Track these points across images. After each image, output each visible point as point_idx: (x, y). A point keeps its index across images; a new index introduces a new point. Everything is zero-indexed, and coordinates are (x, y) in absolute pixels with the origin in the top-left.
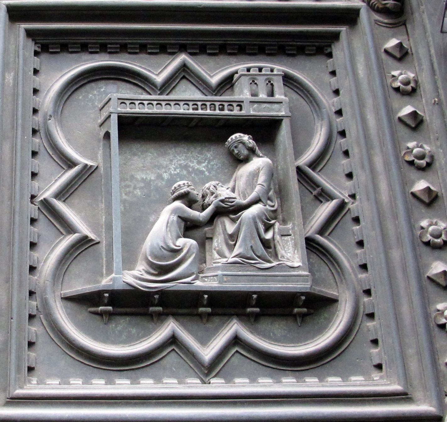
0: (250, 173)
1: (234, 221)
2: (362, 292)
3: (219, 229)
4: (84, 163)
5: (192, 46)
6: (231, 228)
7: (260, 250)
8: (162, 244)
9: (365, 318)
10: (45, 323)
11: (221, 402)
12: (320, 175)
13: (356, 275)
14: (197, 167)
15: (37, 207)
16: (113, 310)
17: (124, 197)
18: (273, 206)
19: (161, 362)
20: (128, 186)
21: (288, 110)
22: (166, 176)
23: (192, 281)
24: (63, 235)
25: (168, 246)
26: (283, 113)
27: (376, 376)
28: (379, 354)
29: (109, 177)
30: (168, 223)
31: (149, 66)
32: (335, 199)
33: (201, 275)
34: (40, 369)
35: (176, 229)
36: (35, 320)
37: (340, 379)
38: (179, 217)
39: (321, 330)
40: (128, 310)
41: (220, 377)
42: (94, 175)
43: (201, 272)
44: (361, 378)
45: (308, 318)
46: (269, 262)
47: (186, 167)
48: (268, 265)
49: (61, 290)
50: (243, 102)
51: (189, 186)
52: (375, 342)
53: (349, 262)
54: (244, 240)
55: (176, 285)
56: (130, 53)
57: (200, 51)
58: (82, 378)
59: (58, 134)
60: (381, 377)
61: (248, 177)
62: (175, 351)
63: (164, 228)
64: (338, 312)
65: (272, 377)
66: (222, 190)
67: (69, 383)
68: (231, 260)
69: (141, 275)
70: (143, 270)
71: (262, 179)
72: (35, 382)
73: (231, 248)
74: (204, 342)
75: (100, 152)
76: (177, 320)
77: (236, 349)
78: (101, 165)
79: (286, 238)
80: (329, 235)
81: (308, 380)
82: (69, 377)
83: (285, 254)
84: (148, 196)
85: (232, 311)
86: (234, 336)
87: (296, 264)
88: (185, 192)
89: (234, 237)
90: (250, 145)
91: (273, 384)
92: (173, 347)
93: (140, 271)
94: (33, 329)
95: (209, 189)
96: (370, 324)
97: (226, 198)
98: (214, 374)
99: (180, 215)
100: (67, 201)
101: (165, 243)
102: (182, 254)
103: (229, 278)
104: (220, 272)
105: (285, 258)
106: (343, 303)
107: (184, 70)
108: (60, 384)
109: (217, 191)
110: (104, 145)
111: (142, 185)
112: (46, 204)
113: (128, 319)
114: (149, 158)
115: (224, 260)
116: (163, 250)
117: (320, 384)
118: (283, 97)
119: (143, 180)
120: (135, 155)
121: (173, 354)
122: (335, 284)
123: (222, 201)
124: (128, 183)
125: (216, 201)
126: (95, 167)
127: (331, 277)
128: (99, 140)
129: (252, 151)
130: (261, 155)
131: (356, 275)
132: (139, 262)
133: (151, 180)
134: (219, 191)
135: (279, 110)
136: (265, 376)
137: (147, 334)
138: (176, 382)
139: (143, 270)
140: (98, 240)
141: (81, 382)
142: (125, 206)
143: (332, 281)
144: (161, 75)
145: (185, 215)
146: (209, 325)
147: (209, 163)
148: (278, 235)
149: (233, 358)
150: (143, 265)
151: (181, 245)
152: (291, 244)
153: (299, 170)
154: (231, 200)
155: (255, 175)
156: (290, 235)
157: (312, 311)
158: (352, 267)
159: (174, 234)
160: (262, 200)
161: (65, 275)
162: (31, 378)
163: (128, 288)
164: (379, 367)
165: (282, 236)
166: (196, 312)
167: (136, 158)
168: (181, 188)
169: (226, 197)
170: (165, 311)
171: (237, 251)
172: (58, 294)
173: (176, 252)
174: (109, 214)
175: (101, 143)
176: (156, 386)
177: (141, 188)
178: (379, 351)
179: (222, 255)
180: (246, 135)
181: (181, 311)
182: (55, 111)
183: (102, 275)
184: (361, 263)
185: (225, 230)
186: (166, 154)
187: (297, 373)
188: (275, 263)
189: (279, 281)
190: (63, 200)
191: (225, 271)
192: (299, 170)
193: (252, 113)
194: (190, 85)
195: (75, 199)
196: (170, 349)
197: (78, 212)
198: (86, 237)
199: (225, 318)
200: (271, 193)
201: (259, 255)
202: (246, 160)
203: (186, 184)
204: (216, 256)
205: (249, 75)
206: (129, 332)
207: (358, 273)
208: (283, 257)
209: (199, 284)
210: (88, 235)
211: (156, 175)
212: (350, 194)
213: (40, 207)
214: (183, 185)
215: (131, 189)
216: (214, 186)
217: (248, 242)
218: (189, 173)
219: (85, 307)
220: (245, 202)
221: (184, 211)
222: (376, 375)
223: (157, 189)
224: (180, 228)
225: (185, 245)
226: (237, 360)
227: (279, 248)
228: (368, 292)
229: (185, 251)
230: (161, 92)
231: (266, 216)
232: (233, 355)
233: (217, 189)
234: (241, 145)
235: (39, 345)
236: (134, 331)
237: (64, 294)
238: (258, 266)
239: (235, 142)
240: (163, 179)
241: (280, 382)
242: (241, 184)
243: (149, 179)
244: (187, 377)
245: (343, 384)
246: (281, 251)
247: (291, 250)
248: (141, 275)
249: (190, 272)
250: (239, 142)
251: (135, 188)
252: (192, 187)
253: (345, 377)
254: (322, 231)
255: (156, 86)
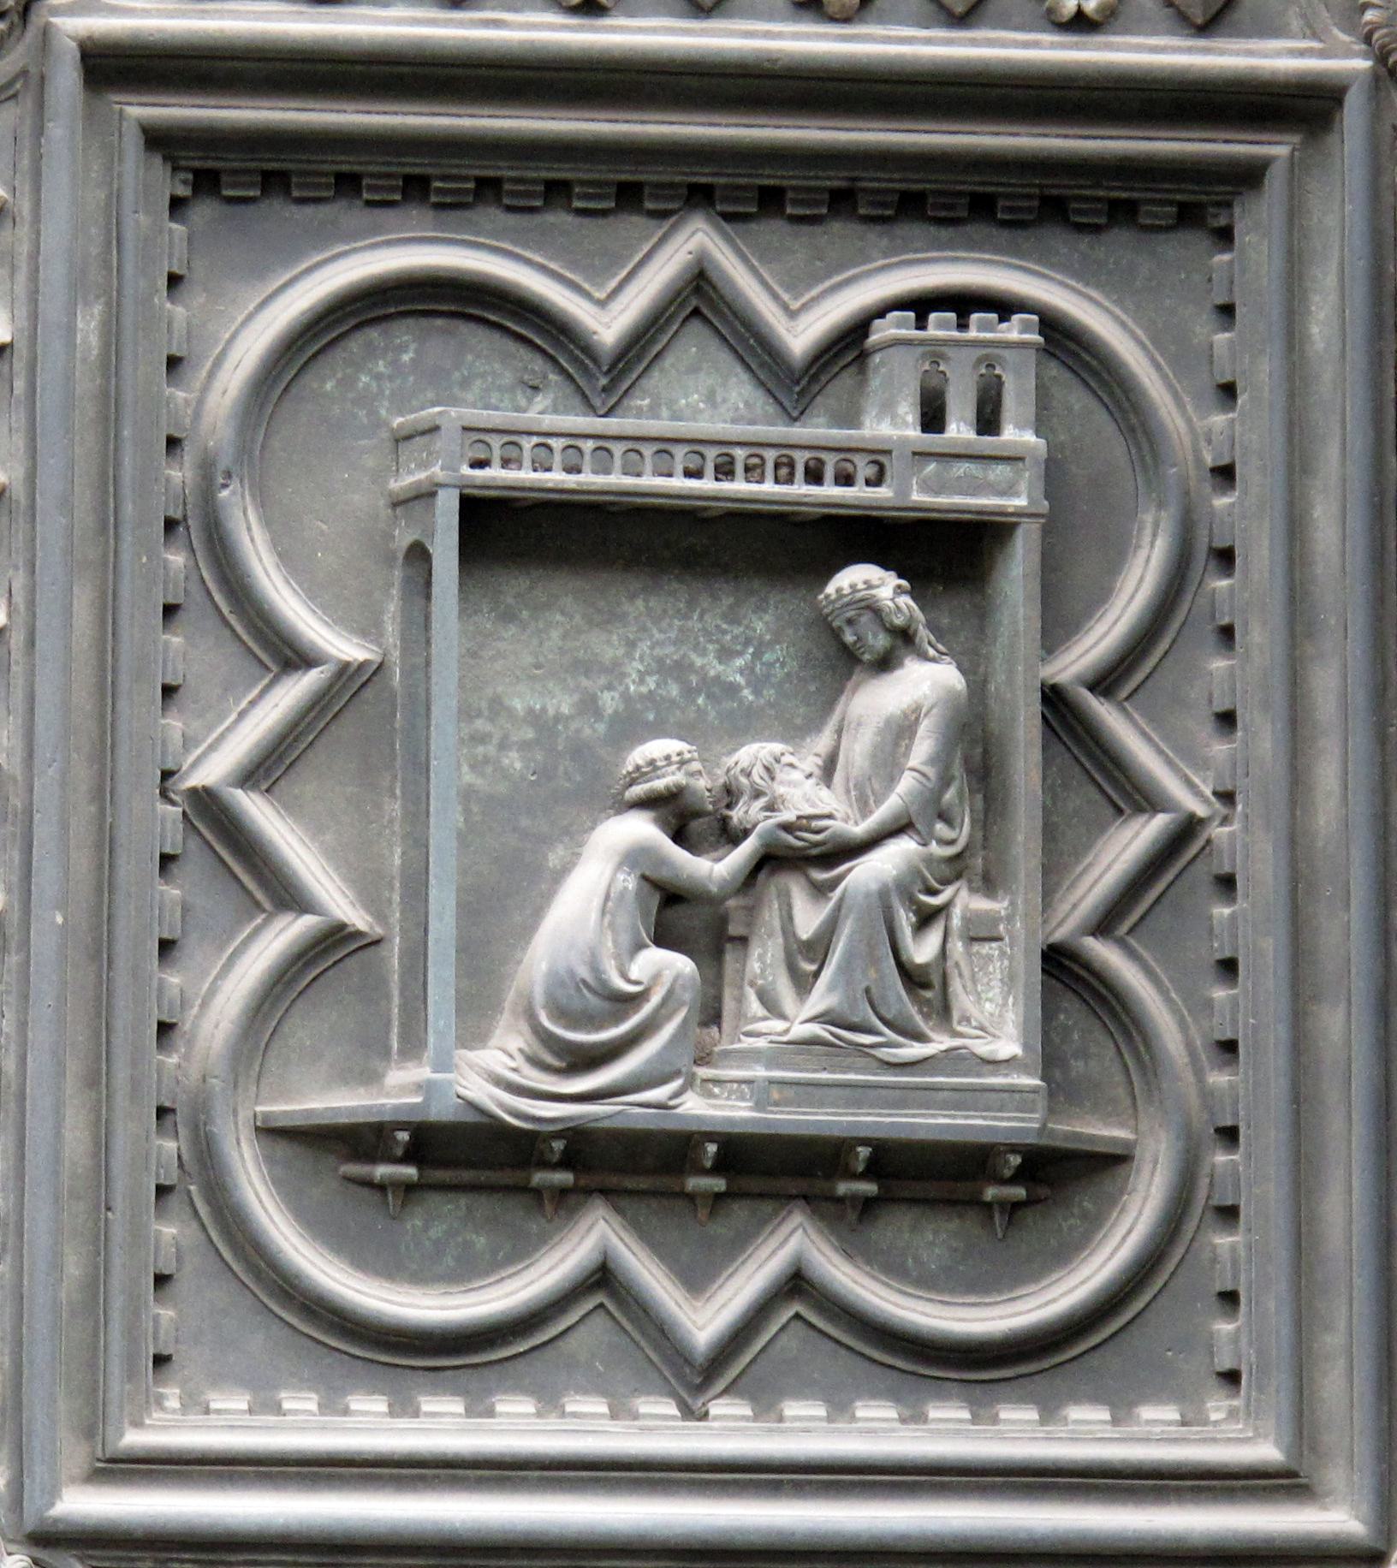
0: (888, 722)
1: (821, 891)
2: (1212, 1131)
3: (771, 915)
4: (340, 661)
5: (734, 193)
6: (808, 918)
7: (892, 999)
8: (583, 972)
9: (1209, 1215)
10: (203, 1210)
11: (736, 1482)
12: (1130, 709)
13: (1199, 1074)
14: (715, 668)
15: (180, 809)
16: (421, 1176)
17: (468, 777)
18: (951, 842)
19: (560, 1343)
20: (480, 739)
21: (1039, 493)
22: (610, 702)
23: (671, 1098)
24: (264, 911)
25: (604, 983)
26: (1021, 502)
27: (1218, 1409)
28: (1235, 1338)
29: (421, 707)
30: (607, 898)
31: (573, 265)
32: (1163, 811)
33: (703, 1072)
34: (188, 1359)
35: (630, 920)
36: (174, 1201)
37: (1104, 1414)
38: (644, 878)
39: (1063, 1254)
40: (467, 1176)
41: (741, 1394)
42: (368, 693)
43: (703, 1059)
44: (1170, 1413)
45: (1029, 1216)
46: (920, 1037)
47: (679, 670)
48: (915, 1050)
49: (256, 1103)
50: (888, 452)
51: (682, 763)
52: (1230, 1298)
53: (1183, 1026)
54: (846, 968)
55: (620, 1112)
56: (510, 209)
57: (760, 207)
58: (317, 1391)
59: (252, 540)
60: (1232, 1414)
61: (880, 732)
62: (609, 1313)
63: (594, 916)
64: (1125, 1197)
65: (894, 1396)
66: (790, 783)
67: (277, 1409)
68: (801, 1030)
69: (515, 1070)
70: (521, 1050)
71: (922, 749)
72: (173, 1403)
73: (803, 984)
74: (696, 1280)
75: (392, 607)
76: (619, 1210)
77: (796, 1307)
78: (396, 655)
79: (986, 949)
80: (1131, 931)
81: (1008, 1413)
82: (276, 1387)
83: (973, 1010)
84: (545, 773)
85: (793, 1186)
86: (791, 1271)
87: (1008, 1047)
88: (667, 788)
89: (818, 948)
90: (899, 621)
91: (897, 1425)
92: (600, 1298)
93: (511, 1056)
94: (169, 1231)
95: (749, 775)
96: (1223, 1241)
97: (799, 818)
98: (721, 1385)
99: (647, 873)
100: (276, 789)
101: (596, 969)
102: (647, 1009)
103: (790, 1092)
104: (760, 1072)
105: (974, 1023)
106: (1145, 1173)
107: (698, 290)
108: (251, 1411)
109: (775, 785)
110: (407, 581)
111: (530, 734)
112: (207, 805)
113: (463, 1200)
114: (555, 634)
115: (778, 1025)
116: (585, 991)
117: (1042, 1431)
118: (1029, 437)
119: (534, 718)
120: (508, 617)
121: (599, 1320)
122: (1128, 1102)
123: (787, 827)
124: (480, 724)
125: (767, 824)
126: (375, 667)
127: (1119, 1078)
128: (389, 559)
129: (904, 637)
130: (931, 652)
131: (1199, 1074)
132: (505, 1019)
133: (558, 718)
134: (781, 783)
135: (1009, 490)
136: (874, 1394)
137: (520, 1251)
138: (604, 1409)
139: (521, 1050)
140: (379, 931)
141: (312, 1406)
142: (467, 811)
143: (1121, 1092)
144: (616, 306)
145: (664, 874)
146: (720, 1229)
147: (757, 655)
148: (961, 937)
149: (784, 1339)
150: (521, 1034)
151: (645, 980)
152: (997, 968)
153: (1054, 699)
154: (815, 824)
155: (902, 730)
156: (998, 939)
157: (1043, 1191)
158: (1189, 1045)
159: (625, 939)
160: (918, 826)
161: (270, 1053)
162: (161, 1390)
163: (471, 1117)
164: (1231, 1378)
165: (974, 939)
166: (677, 1189)
167: (513, 629)
168: (659, 772)
169: (801, 813)
170: (582, 1182)
171: (821, 998)
172: (244, 1115)
173: (625, 1002)
174: (418, 843)
175: (398, 574)
176: (540, 1424)
177: (524, 746)
178: (1238, 1329)
179: (772, 1007)
180: (892, 573)
181: (630, 1183)
182: (244, 449)
183: (386, 1053)
184: (1219, 1036)
185: (788, 919)
186: (613, 618)
187: (978, 1389)
188: (940, 1043)
189: (945, 1105)
190: (264, 787)
191: (779, 1066)
192: (1054, 699)
193: (917, 497)
194: (714, 344)
195: (305, 784)
196: (589, 1304)
197: (314, 827)
198: (342, 926)
199: (767, 1207)
200: (950, 795)
201: (889, 1016)
202: (885, 664)
203: (675, 758)
204: (755, 1006)
205: (923, 342)
206: (467, 1245)
207: (1207, 1068)
208: (966, 1019)
209: (696, 1107)
210: (346, 920)
211: (576, 697)
212: (1220, 789)
213: (188, 810)
214: (664, 763)
215: (491, 749)
216: (767, 769)
217: (858, 975)
218: (689, 693)
219: (332, 1160)
220: (859, 829)
221: (662, 861)
222: (1217, 1406)
223: (579, 751)
224: (645, 914)
225: (656, 977)
226: (792, 1342)
227: (956, 986)
228: (1229, 1135)
229: (655, 999)
230: (612, 380)
231: (924, 880)
232: (783, 1328)
233: (773, 779)
234: (866, 618)
235: (183, 1286)
236: (481, 1242)
237: (266, 1115)
238: (883, 1053)
239: (848, 604)
240: (597, 713)
241: (919, 1418)
242: (858, 752)
243: (551, 712)
244: (636, 1392)
245: (1110, 1432)
246: (962, 1000)
247: (996, 991)
248: (515, 1070)
249: (668, 1069)
250: (863, 604)
251: (503, 746)
252: (696, 766)
253: (1122, 1409)
254: (1105, 924)
255: (595, 360)
